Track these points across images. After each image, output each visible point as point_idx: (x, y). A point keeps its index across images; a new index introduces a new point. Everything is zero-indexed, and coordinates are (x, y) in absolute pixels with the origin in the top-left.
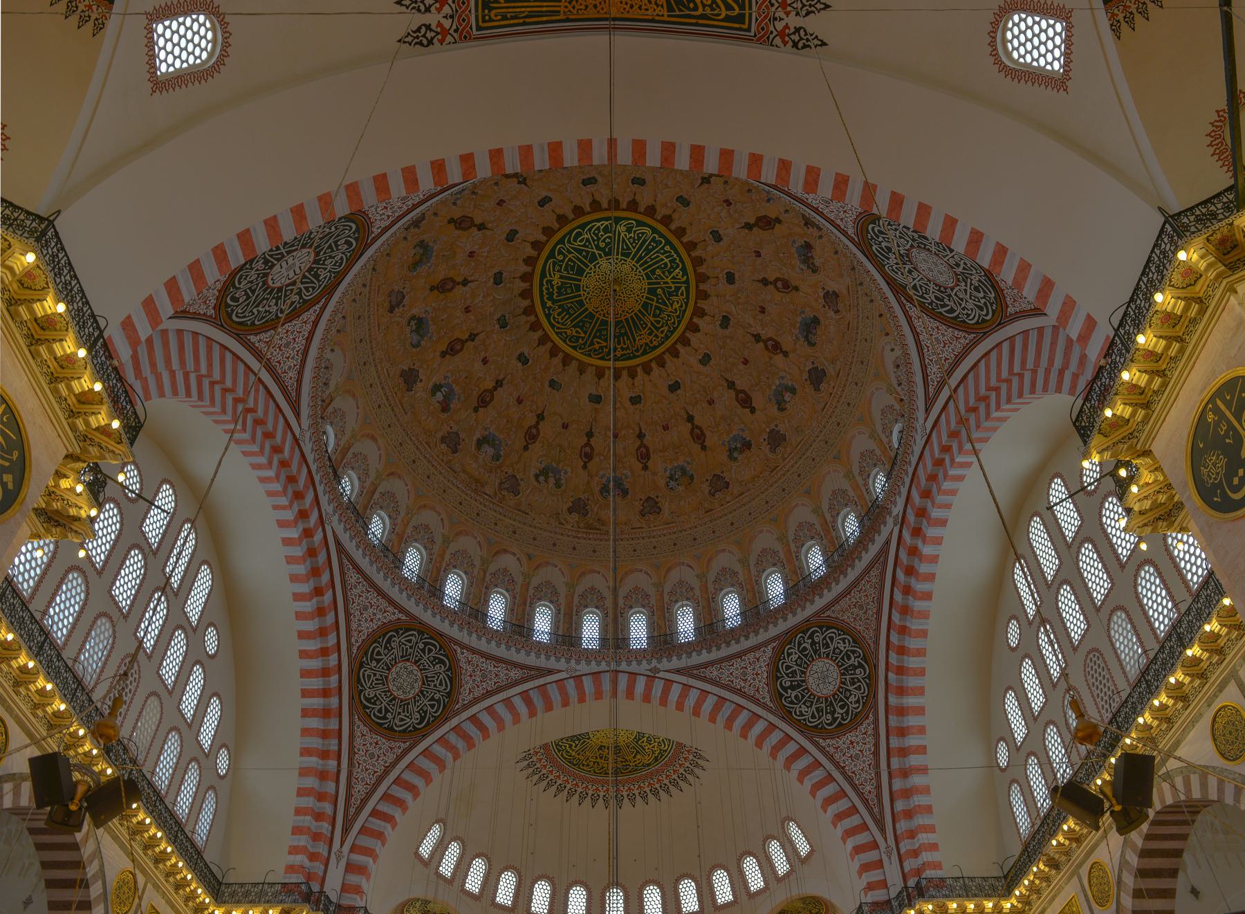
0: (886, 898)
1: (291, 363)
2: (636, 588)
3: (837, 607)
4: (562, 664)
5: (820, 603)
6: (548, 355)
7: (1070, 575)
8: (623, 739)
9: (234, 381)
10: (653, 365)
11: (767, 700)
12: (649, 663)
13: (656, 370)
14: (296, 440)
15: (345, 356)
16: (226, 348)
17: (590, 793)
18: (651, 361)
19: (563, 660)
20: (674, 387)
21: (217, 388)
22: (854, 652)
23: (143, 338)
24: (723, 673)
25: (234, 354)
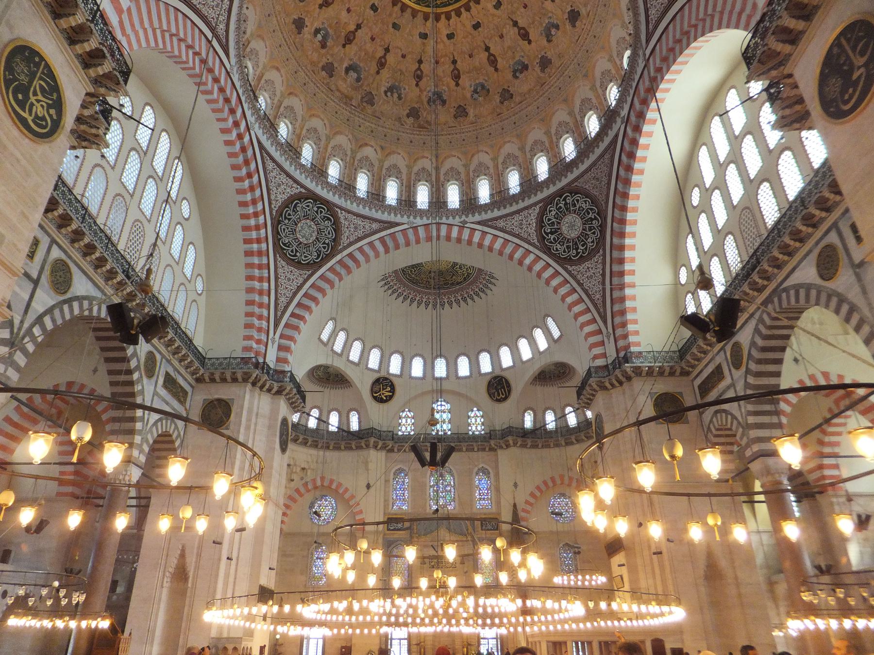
0: (605, 364)
1: (221, 18)
2: (452, 168)
3: (581, 180)
4: (405, 219)
5: (571, 177)
6: (391, 4)
7: (736, 158)
8: (443, 267)
9: (185, 34)
10: (463, 10)
11: (536, 241)
12: (460, 217)
13: (464, 14)
14: (228, 73)
15: (255, 10)
16: (178, 10)
17: (424, 300)
18: (460, 7)
19: (405, 216)
20: (477, 26)
21: (175, 39)
22: (591, 209)
23: (125, 8)
24: (507, 224)
25: (183, 14)
